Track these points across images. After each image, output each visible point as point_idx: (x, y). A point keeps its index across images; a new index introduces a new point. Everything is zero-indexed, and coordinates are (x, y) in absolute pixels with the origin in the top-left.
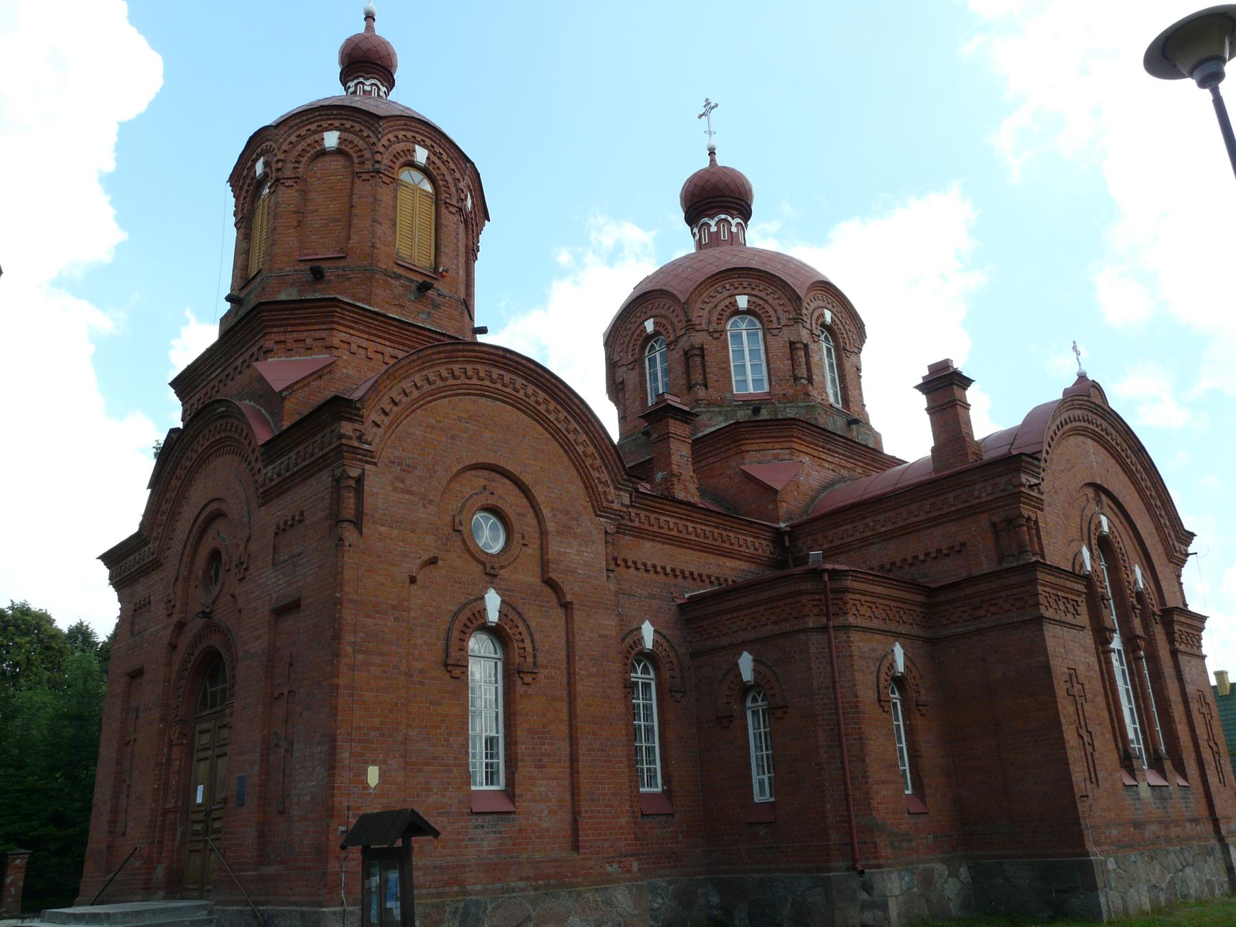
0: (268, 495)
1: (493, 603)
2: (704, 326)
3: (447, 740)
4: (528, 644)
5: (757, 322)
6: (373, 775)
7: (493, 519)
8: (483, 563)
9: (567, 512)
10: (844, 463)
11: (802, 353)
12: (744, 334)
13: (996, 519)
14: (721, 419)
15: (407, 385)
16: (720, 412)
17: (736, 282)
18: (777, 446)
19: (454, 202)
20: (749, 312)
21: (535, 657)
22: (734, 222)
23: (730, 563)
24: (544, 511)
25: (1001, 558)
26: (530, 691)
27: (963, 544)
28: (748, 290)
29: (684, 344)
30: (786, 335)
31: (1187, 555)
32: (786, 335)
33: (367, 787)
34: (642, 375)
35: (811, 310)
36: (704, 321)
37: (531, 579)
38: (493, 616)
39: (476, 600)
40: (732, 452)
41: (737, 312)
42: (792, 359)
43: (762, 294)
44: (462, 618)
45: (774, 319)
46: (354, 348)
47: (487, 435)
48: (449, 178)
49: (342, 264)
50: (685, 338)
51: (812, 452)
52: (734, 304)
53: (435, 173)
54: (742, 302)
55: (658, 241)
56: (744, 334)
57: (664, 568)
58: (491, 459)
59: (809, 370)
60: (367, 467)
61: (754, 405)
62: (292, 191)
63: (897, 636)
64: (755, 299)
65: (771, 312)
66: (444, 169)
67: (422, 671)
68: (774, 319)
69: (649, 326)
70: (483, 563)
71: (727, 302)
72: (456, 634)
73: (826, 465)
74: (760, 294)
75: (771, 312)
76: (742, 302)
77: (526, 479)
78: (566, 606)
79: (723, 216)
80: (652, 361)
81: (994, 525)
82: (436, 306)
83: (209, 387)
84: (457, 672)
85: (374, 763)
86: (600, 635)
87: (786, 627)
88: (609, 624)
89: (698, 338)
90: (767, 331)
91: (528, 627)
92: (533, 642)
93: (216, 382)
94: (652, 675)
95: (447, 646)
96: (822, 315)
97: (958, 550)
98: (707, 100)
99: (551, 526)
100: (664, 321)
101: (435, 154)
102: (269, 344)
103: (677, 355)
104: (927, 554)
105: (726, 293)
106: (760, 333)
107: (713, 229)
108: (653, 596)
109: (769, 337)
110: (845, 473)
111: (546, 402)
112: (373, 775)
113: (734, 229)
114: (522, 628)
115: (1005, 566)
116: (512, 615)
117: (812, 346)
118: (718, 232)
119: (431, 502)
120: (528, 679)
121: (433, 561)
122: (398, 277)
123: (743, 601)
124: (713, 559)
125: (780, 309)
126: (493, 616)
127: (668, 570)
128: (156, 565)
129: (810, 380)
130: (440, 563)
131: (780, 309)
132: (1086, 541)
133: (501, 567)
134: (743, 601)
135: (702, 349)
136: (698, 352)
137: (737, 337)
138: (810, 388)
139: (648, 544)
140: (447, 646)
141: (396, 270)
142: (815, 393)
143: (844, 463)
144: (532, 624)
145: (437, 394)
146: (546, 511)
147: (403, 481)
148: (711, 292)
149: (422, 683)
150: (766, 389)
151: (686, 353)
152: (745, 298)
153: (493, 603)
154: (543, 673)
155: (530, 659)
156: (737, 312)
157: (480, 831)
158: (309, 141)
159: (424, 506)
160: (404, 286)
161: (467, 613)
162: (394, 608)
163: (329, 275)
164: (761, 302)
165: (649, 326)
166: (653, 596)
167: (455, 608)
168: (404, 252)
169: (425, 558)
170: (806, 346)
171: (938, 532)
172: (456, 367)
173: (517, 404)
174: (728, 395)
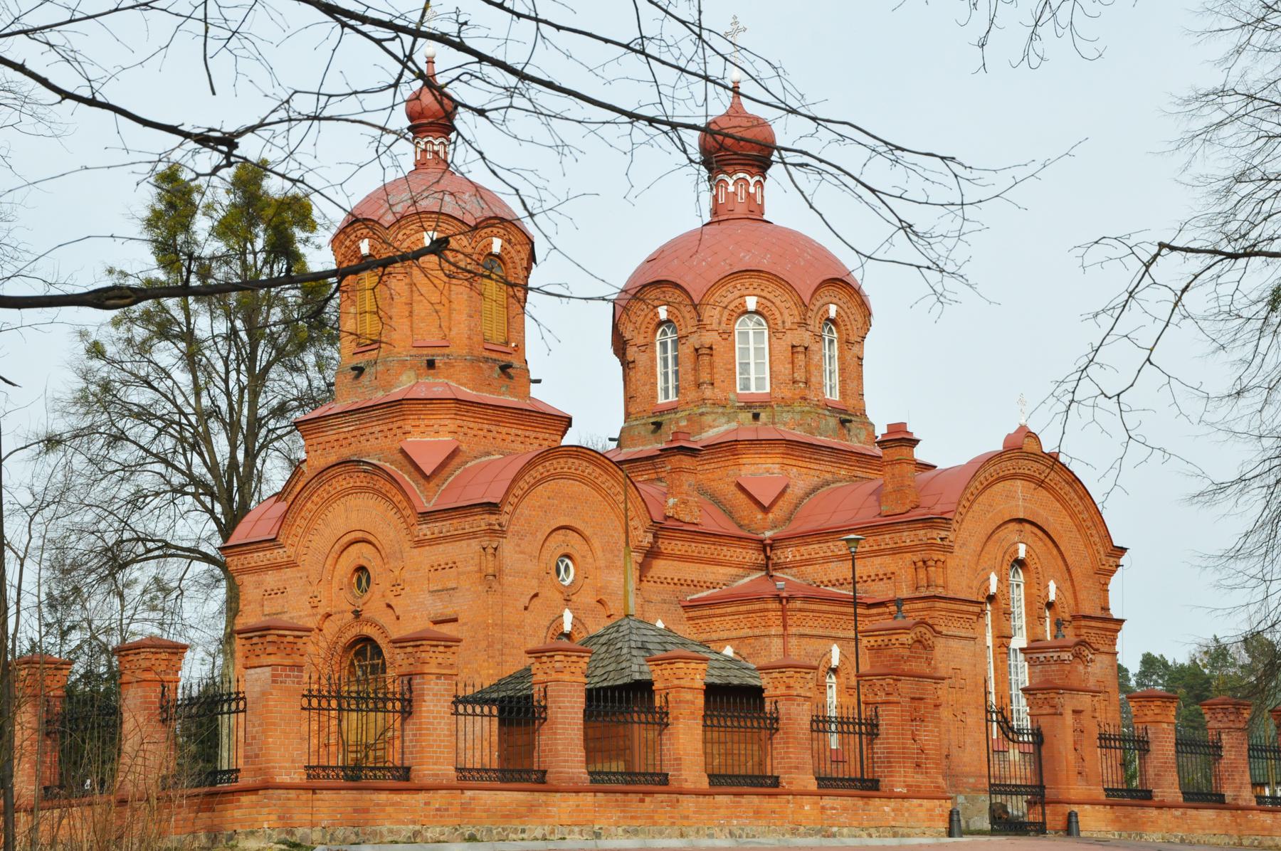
0: (419, 543)
2: (715, 326)
5: (763, 322)
7: (567, 561)
9: (612, 551)
10: (830, 469)
11: (801, 357)
12: (751, 333)
13: (915, 559)
14: (723, 420)
15: (521, 484)
16: (723, 414)
17: (747, 281)
18: (769, 461)
20: (756, 312)
22: (752, 181)
23: (722, 570)
28: (758, 291)
29: (694, 341)
31: (1118, 566)
34: (653, 359)
35: (815, 309)
36: (715, 321)
40: (730, 463)
41: (746, 312)
42: (793, 363)
43: (770, 296)
45: (780, 322)
46: (465, 430)
48: (517, 259)
49: (447, 351)
50: (696, 335)
51: (800, 464)
52: (743, 304)
54: (751, 303)
55: (672, 201)
56: (751, 333)
59: (807, 371)
61: (754, 408)
62: (400, 283)
63: (836, 639)
64: (764, 301)
65: (778, 315)
66: (513, 253)
71: (736, 303)
73: (812, 472)
74: (768, 296)
76: (751, 303)
77: (587, 533)
79: (741, 175)
82: (510, 377)
83: (342, 436)
87: (757, 632)
89: (709, 338)
90: (773, 332)
93: (348, 435)
97: (889, 577)
98: (735, 17)
102: (408, 428)
103: (686, 350)
105: (737, 293)
106: (766, 332)
107: (731, 189)
108: (664, 601)
109: (774, 339)
110: (828, 476)
113: (752, 190)
115: (917, 595)
117: (814, 347)
118: (735, 194)
121: (536, 595)
122: (486, 360)
123: (729, 610)
124: (710, 569)
125: (786, 312)
128: (292, 564)
131: (786, 312)
132: (998, 568)
134: (729, 610)
135: (711, 348)
136: (708, 351)
137: (745, 335)
141: (487, 354)
142: (811, 396)
143: (830, 469)
145: (538, 482)
146: (599, 554)
148: (723, 291)
150: (768, 390)
152: (755, 299)
156: (746, 312)
158: (413, 239)
160: (491, 368)
162: (518, 627)
163: (438, 364)
164: (769, 304)
166: (664, 601)
168: (488, 335)
171: (878, 560)
173: (582, 480)
174: (732, 396)
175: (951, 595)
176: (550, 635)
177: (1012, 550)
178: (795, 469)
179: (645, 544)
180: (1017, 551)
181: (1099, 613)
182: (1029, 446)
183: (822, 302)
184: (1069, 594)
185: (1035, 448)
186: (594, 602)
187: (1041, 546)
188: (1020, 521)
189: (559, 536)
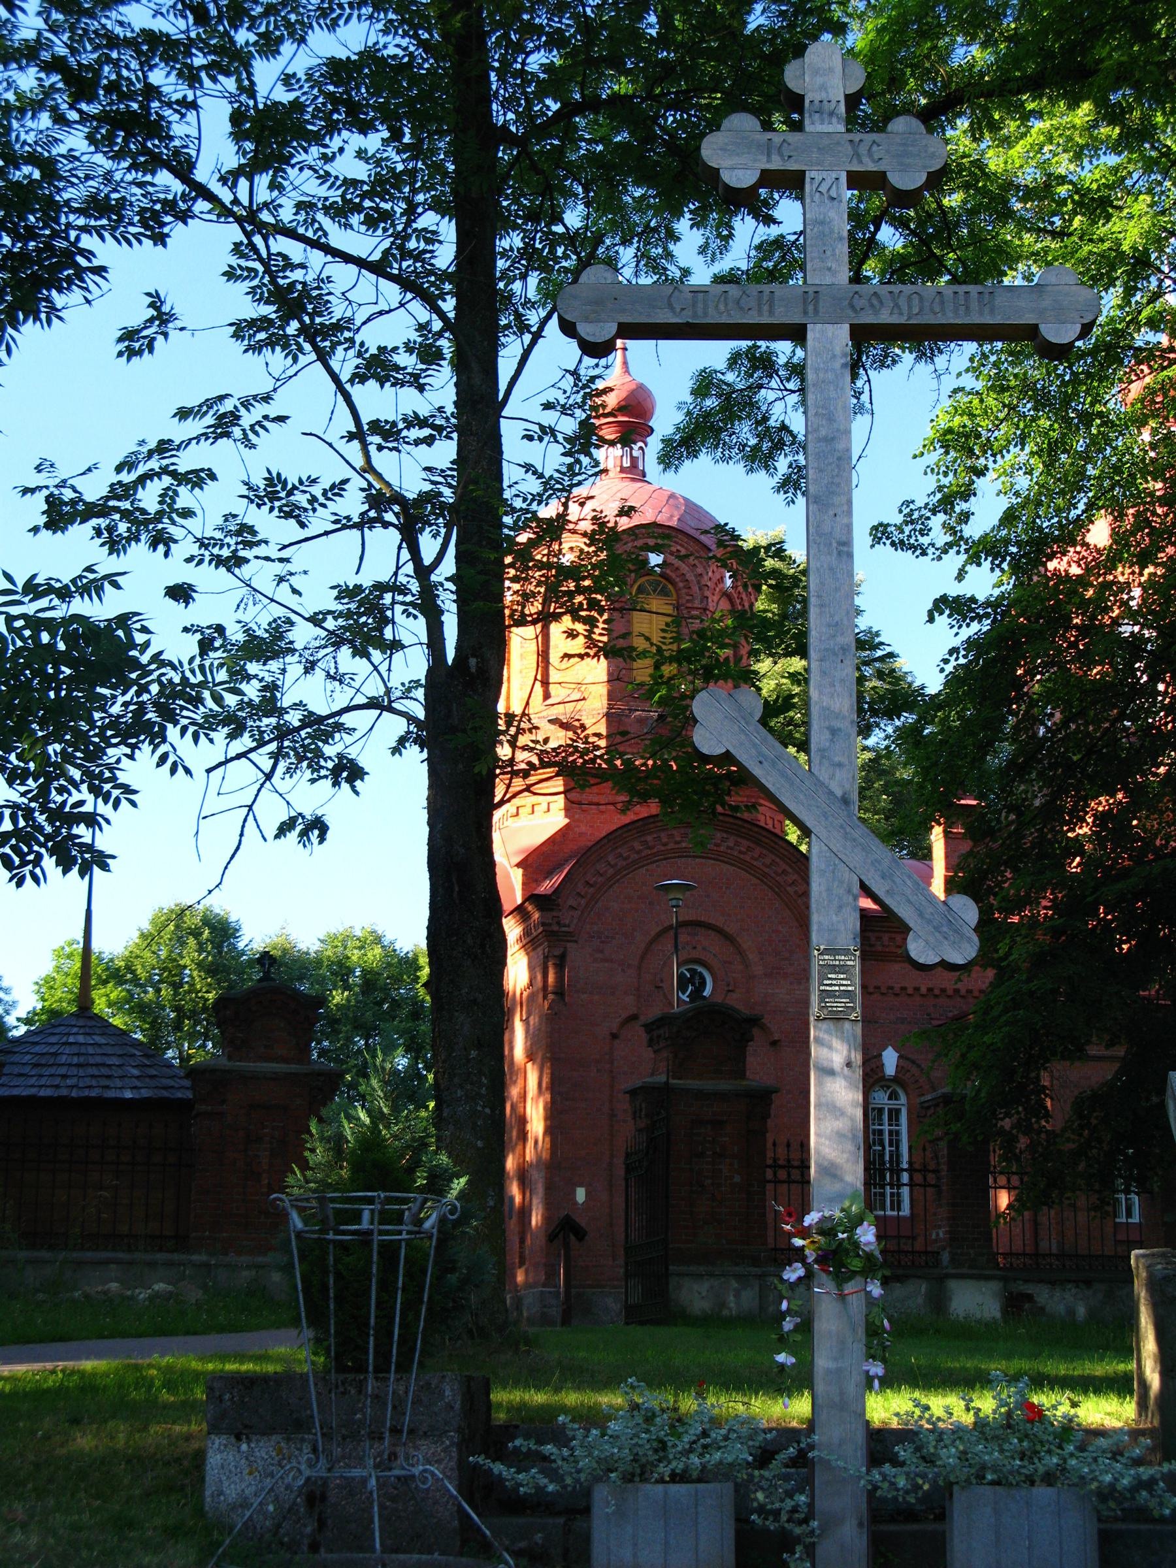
6: (581, 1195)
19: (697, 604)
24: (751, 956)
33: (576, 1203)
48: (690, 577)
53: (673, 575)
57: (917, 989)
60: (569, 945)
66: (684, 568)
77: (731, 929)
85: (581, 1185)
94: (903, 1099)
101: (672, 554)
111: (749, 849)
112: (581, 1195)
146: (752, 957)
147: (602, 952)
169: (625, 1015)
172: (649, 838)
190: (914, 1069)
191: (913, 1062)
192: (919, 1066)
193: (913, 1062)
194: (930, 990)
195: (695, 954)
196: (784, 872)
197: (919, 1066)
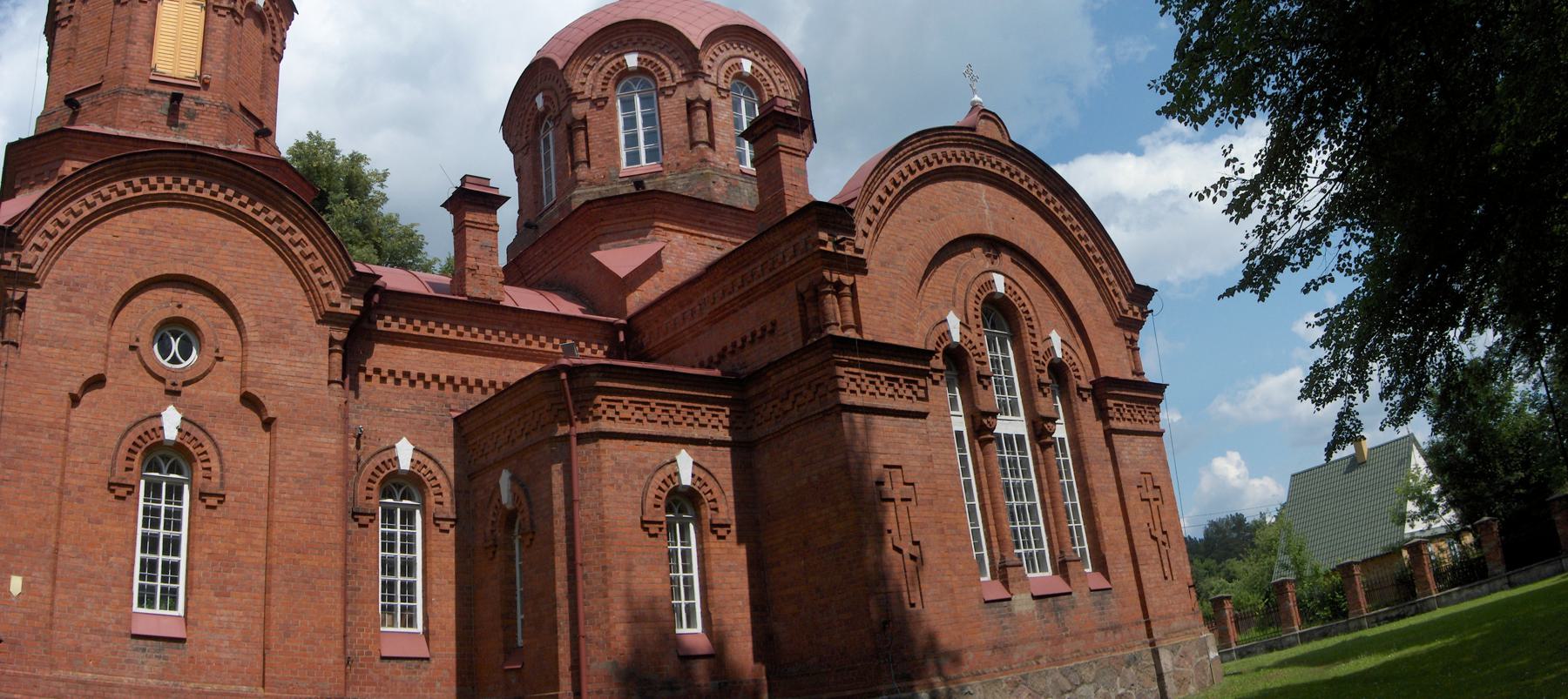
1: (171, 422)
2: (587, 94)
3: (106, 559)
4: (214, 464)
7: (185, 332)
8: (162, 380)
9: (276, 320)
11: (702, 114)
12: (637, 100)
21: (222, 477)
25: (806, 336)
26: (214, 513)
27: (774, 324)
30: (683, 93)
32: (683, 93)
35: (719, 60)
36: (587, 89)
37: (223, 394)
38: (171, 434)
39: (151, 417)
44: (132, 437)
45: (668, 76)
47: (175, 244)
52: (623, 64)
56: (637, 100)
58: (179, 269)
65: (665, 69)
67: (81, 489)
68: (668, 76)
69: (539, 101)
70: (162, 380)
71: (614, 63)
72: (123, 452)
75: (665, 69)
76: (632, 60)
77: (224, 287)
78: (268, 424)
80: (546, 141)
81: (801, 296)
84: (122, 491)
86: (312, 455)
88: (329, 443)
91: (216, 445)
92: (221, 462)
95: (113, 465)
96: (739, 65)
97: (770, 330)
99: (252, 336)
100: (551, 94)
103: (562, 131)
104: (744, 340)
108: (420, 410)
114: (208, 446)
116: (195, 432)
117: (719, 103)
119: (100, 319)
120: (212, 501)
121: (97, 382)
126: (171, 434)
127: (443, 379)
129: (711, 144)
130: (109, 380)
133: (185, 384)
138: (710, 153)
139: (414, 351)
140: (113, 465)
142: (717, 158)
144: (223, 443)
146: (248, 321)
149: (80, 501)
151: (569, 127)
153: (171, 422)
154: (230, 497)
155: (216, 480)
157: (140, 654)
159: (92, 324)
161: (139, 431)
162: (50, 426)
165: (539, 101)
167: (126, 426)
170: (708, 105)
175: (867, 337)
176: (127, 443)
177: (982, 280)
178: (680, 236)
179: (345, 308)
180: (991, 283)
181: (1130, 376)
182: (986, 129)
183: (727, 54)
184: (1083, 353)
185: (997, 136)
186: (237, 397)
187: (1027, 281)
188: (994, 245)
189: (167, 293)
190: (431, 465)
191: (430, 457)
192: (436, 462)
193: (430, 457)
194: (450, 379)
195: (180, 313)
196: (290, 230)
197: (436, 462)
